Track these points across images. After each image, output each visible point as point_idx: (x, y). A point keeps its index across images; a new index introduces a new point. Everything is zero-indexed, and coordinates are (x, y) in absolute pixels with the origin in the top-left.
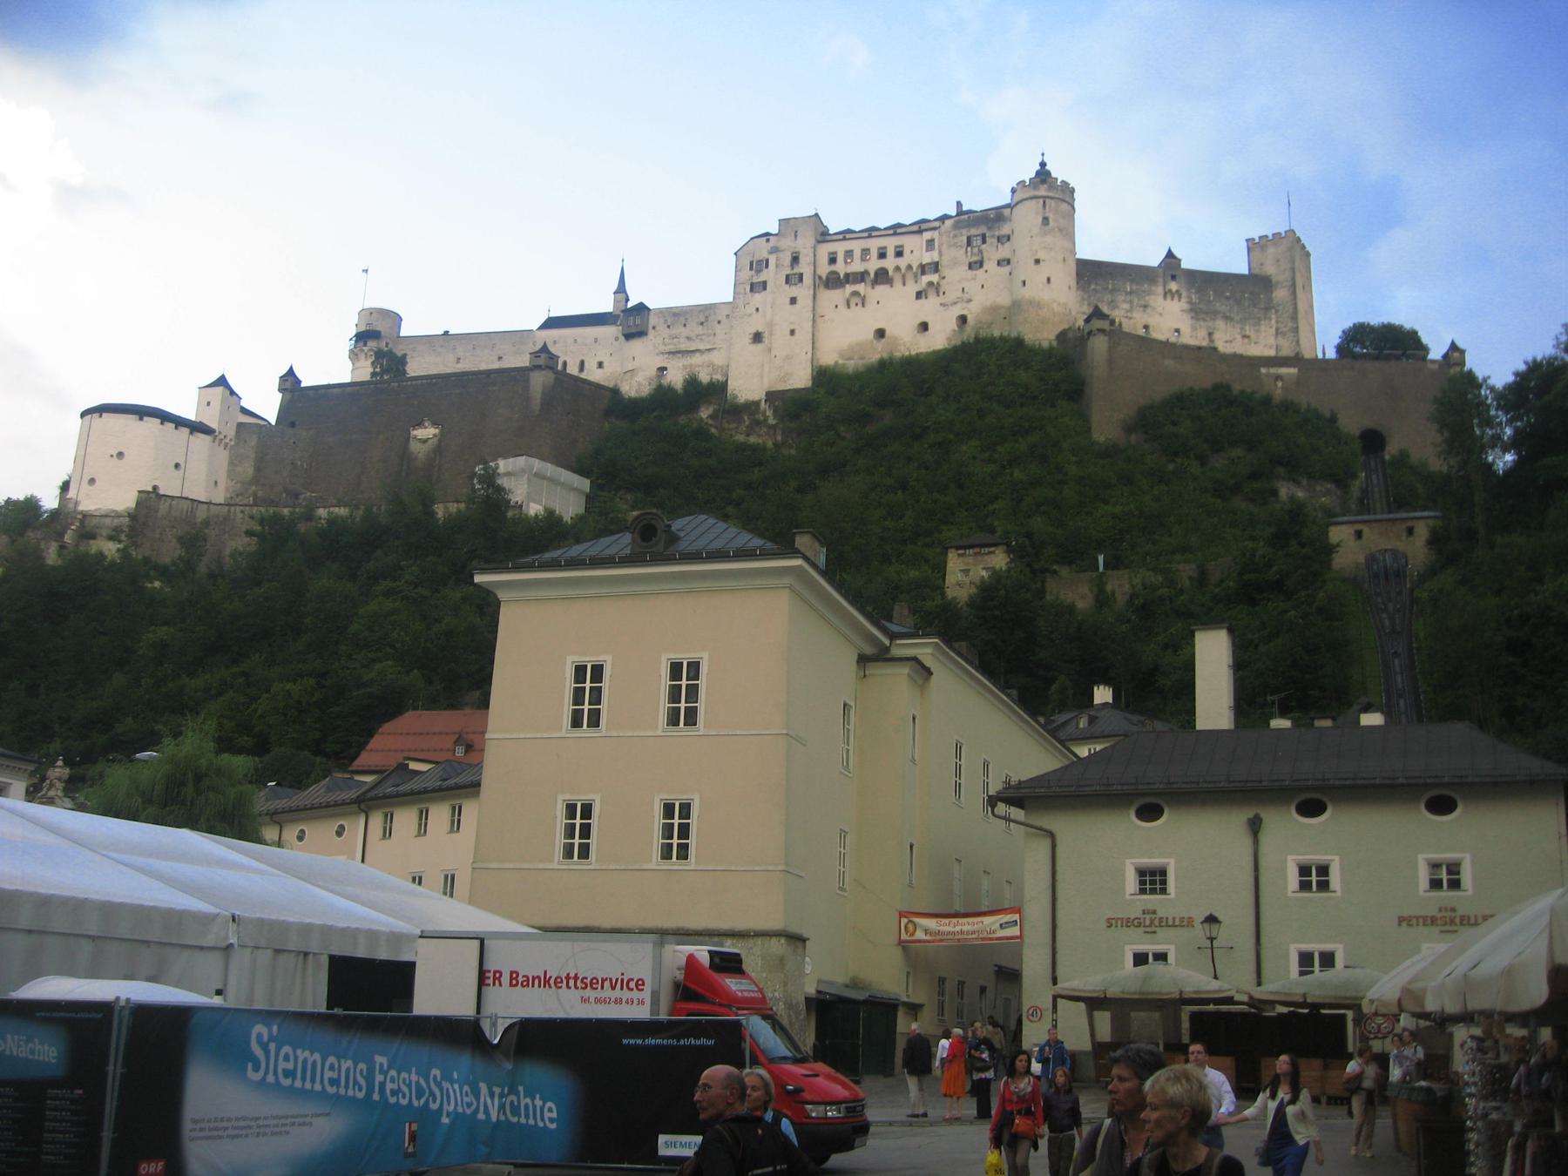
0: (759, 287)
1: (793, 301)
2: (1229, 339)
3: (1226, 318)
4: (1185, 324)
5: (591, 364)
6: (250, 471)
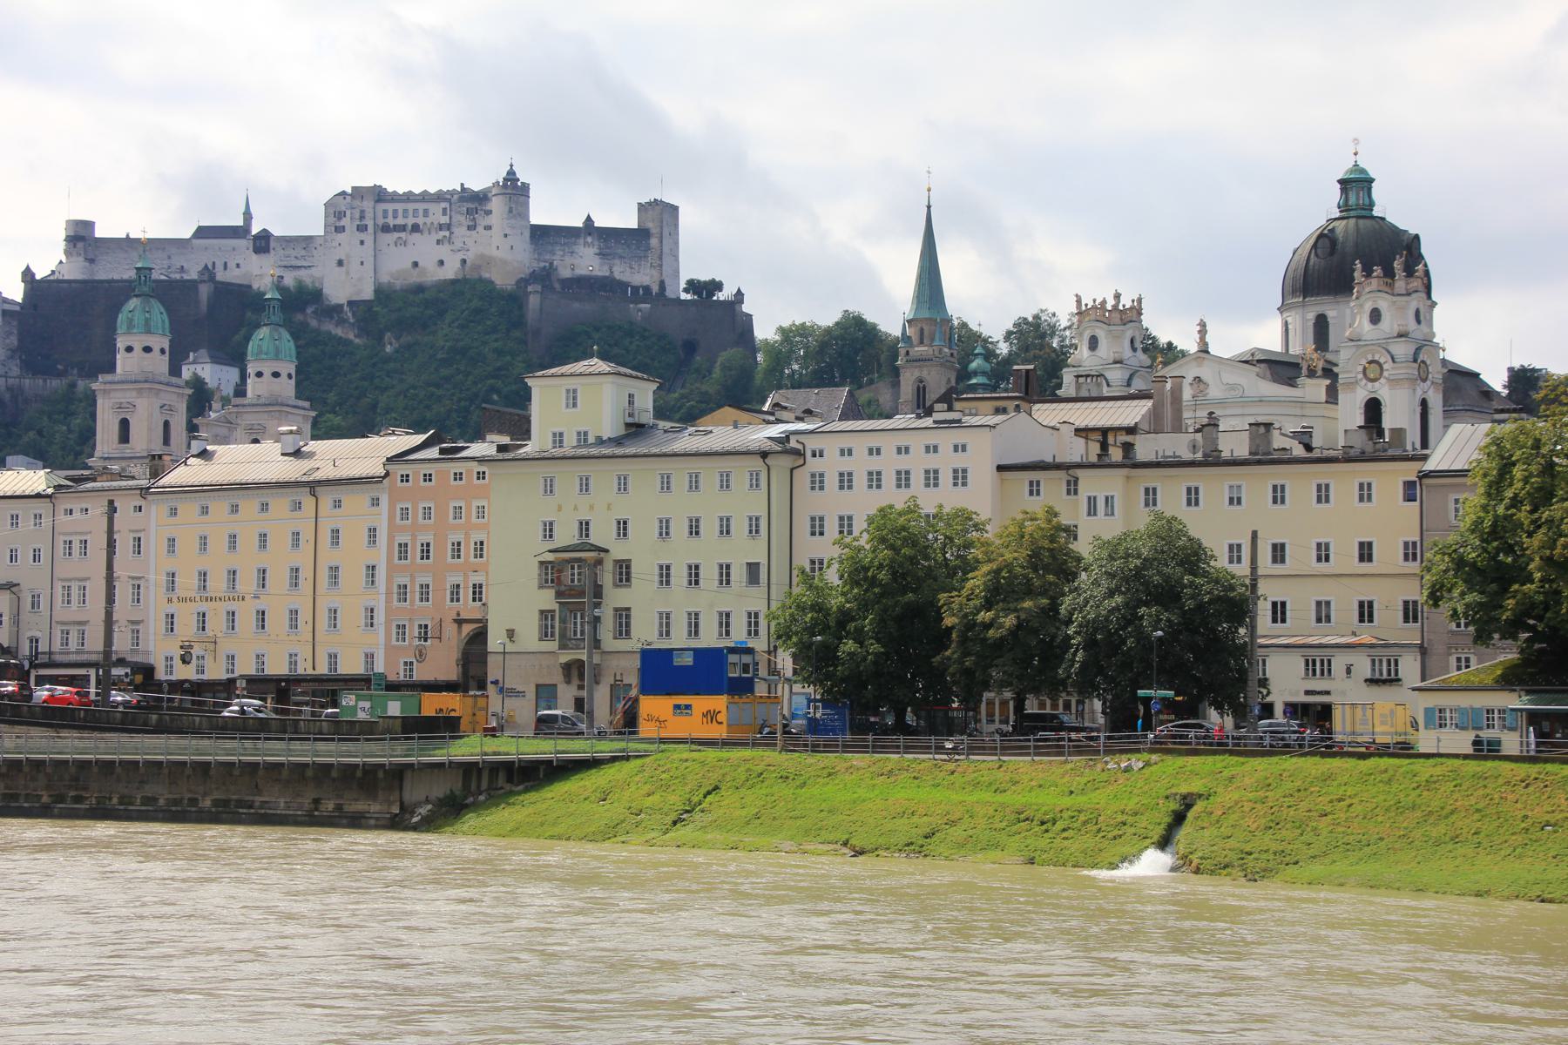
0: (340, 229)
1: (362, 243)
2: (621, 272)
3: (621, 257)
4: (596, 261)
5: (232, 265)
6: (16, 343)
